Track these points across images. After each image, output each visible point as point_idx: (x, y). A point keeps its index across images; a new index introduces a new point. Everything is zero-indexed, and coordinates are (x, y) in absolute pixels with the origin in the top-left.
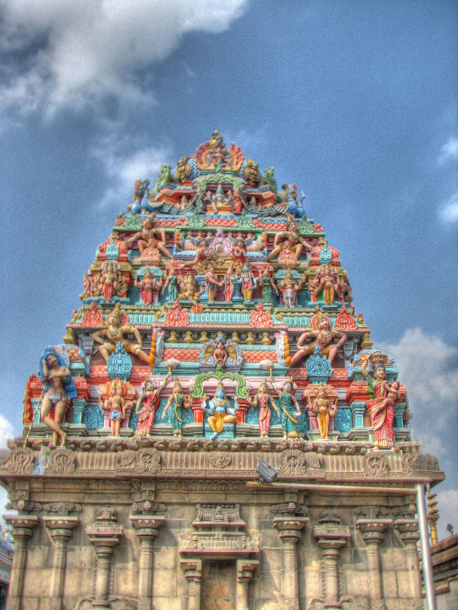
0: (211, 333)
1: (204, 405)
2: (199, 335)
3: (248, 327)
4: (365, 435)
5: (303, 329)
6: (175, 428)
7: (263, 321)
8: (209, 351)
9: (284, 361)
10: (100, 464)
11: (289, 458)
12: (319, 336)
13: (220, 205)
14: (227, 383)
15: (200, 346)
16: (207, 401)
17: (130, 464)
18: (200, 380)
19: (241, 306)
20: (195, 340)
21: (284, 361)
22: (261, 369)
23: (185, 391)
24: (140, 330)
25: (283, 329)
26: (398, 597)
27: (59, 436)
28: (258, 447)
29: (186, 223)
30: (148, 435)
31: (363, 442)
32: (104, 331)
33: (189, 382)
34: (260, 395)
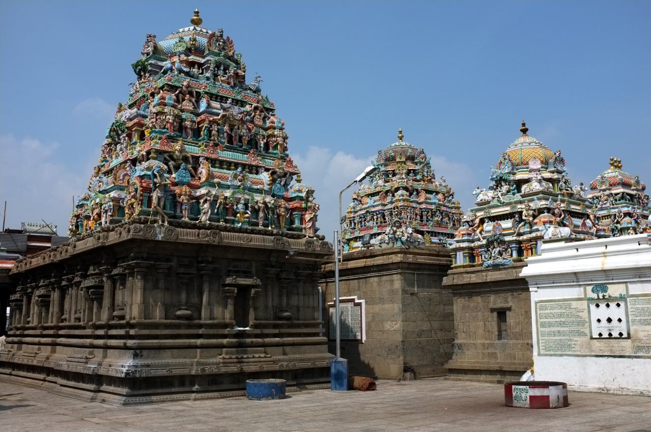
0: (237, 165)
1: (235, 207)
2: (230, 165)
3: (247, 163)
4: (301, 230)
5: (271, 167)
6: (221, 219)
7: (254, 160)
8: (235, 177)
9: (268, 187)
10: (187, 236)
11: (277, 240)
12: (278, 173)
13: (223, 78)
14: (247, 197)
15: (231, 172)
16: (237, 205)
17: (205, 237)
18: (233, 193)
19: (241, 149)
20: (229, 169)
21: (268, 187)
22: (258, 189)
23: (226, 198)
24: (193, 157)
25: (263, 167)
26: (309, 307)
27: (163, 217)
28: (259, 232)
29: (208, 89)
30: (208, 222)
31: (300, 233)
32: (172, 153)
33: (228, 193)
34: (261, 205)
